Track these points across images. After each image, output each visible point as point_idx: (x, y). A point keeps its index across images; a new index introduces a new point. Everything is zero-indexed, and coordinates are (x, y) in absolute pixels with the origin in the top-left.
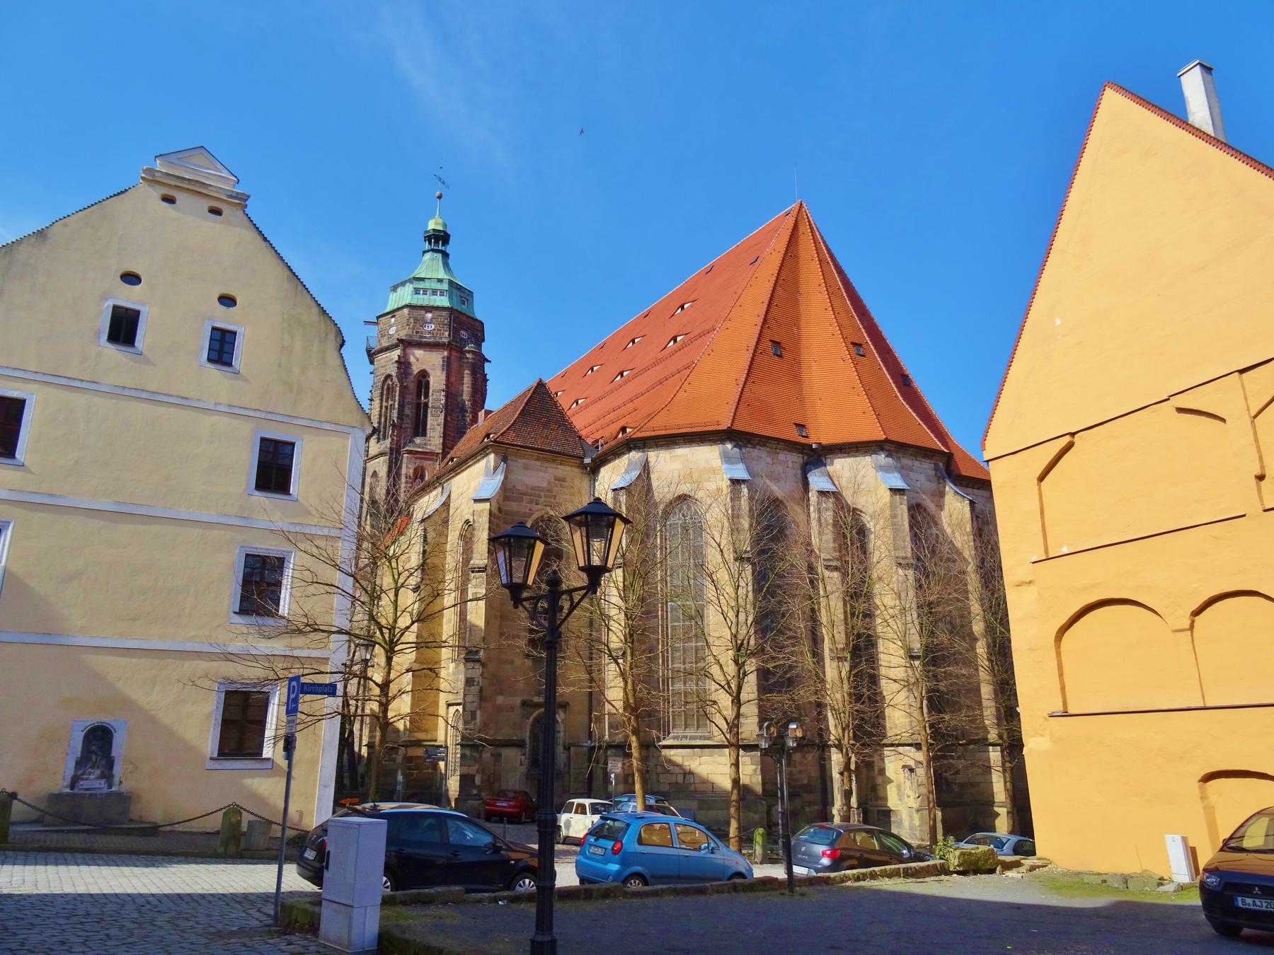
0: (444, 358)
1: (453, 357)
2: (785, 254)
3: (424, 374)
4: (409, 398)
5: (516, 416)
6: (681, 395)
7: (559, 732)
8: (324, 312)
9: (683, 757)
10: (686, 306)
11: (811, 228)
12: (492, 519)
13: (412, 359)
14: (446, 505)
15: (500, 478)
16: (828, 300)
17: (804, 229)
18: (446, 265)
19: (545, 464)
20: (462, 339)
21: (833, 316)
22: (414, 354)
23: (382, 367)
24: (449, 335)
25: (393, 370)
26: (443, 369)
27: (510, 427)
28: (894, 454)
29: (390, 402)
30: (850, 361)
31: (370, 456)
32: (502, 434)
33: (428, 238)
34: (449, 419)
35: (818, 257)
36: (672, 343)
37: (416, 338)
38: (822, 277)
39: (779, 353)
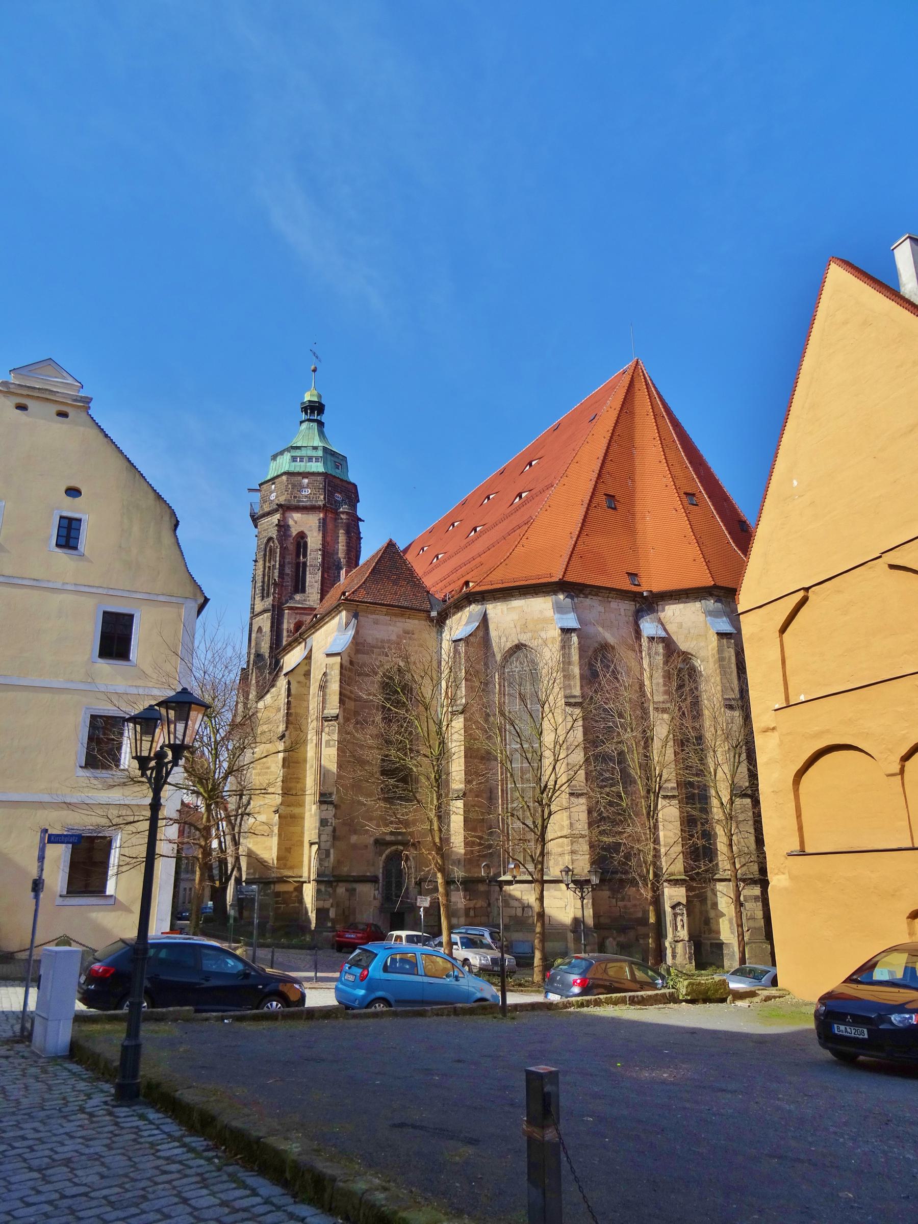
0: (320, 519)
1: (328, 520)
2: (621, 409)
3: (302, 536)
4: (288, 559)
5: (367, 575)
6: (519, 549)
8: (159, 497)
9: (522, 892)
10: (533, 463)
11: (647, 384)
12: (344, 671)
13: (291, 522)
14: (308, 657)
15: (351, 633)
16: (662, 453)
17: (640, 385)
18: (321, 434)
19: (394, 619)
20: (336, 501)
21: (667, 468)
22: (292, 518)
23: (265, 530)
24: (325, 498)
25: (274, 533)
26: (319, 530)
27: (361, 585)
28: (723, 599)
29: (273, 563)
30: (683, 510)
31: (255, 613)
32: (353, 593)
33: (305, 409)
34: (326, 576)
35: (653, 412)
36: (517, 499)
37: (294, 503)
38: (656, 431)
39: (613, 506)
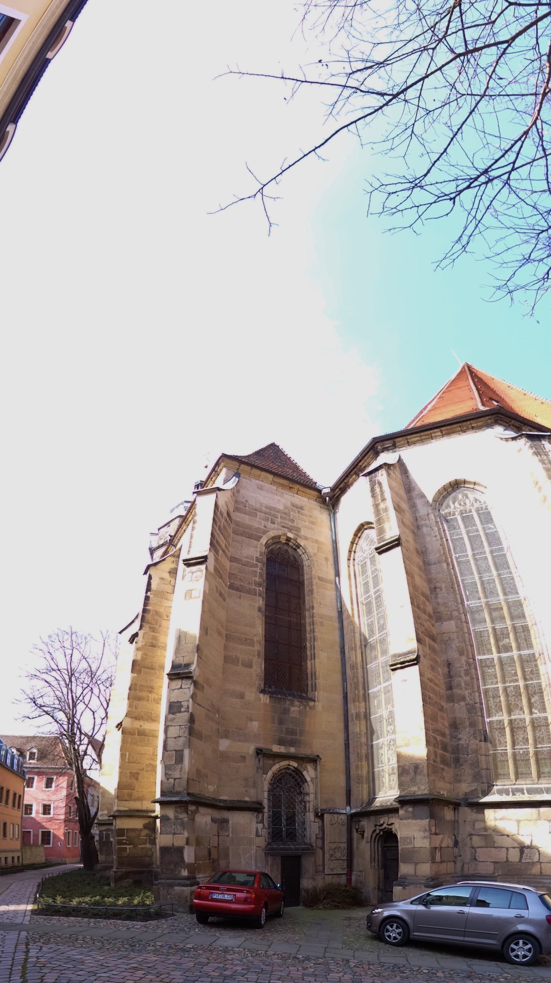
7: (308, 794)
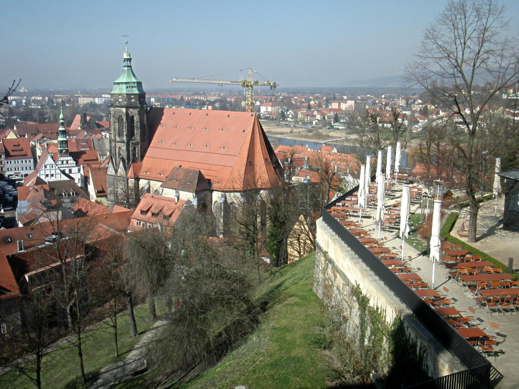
3: (133, 117)
13: (129, 112)
